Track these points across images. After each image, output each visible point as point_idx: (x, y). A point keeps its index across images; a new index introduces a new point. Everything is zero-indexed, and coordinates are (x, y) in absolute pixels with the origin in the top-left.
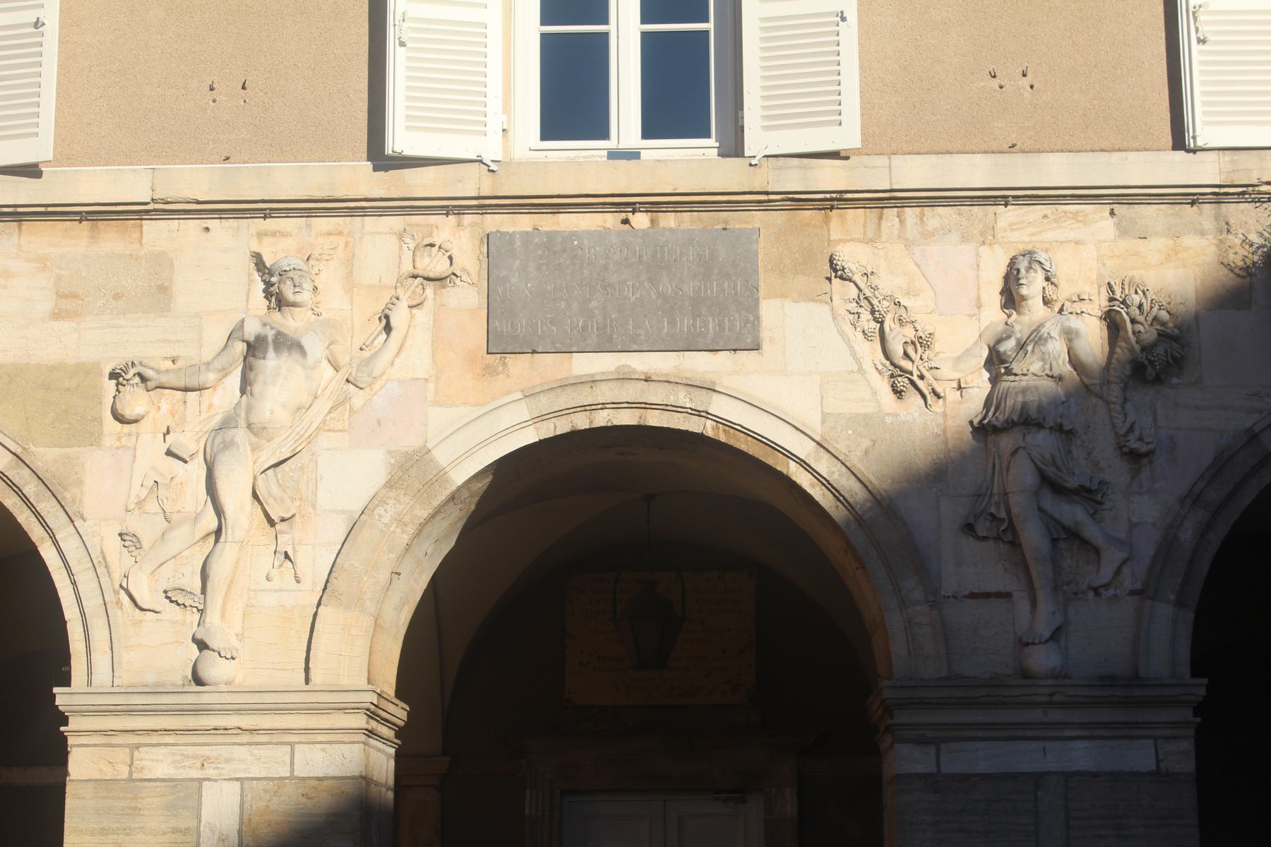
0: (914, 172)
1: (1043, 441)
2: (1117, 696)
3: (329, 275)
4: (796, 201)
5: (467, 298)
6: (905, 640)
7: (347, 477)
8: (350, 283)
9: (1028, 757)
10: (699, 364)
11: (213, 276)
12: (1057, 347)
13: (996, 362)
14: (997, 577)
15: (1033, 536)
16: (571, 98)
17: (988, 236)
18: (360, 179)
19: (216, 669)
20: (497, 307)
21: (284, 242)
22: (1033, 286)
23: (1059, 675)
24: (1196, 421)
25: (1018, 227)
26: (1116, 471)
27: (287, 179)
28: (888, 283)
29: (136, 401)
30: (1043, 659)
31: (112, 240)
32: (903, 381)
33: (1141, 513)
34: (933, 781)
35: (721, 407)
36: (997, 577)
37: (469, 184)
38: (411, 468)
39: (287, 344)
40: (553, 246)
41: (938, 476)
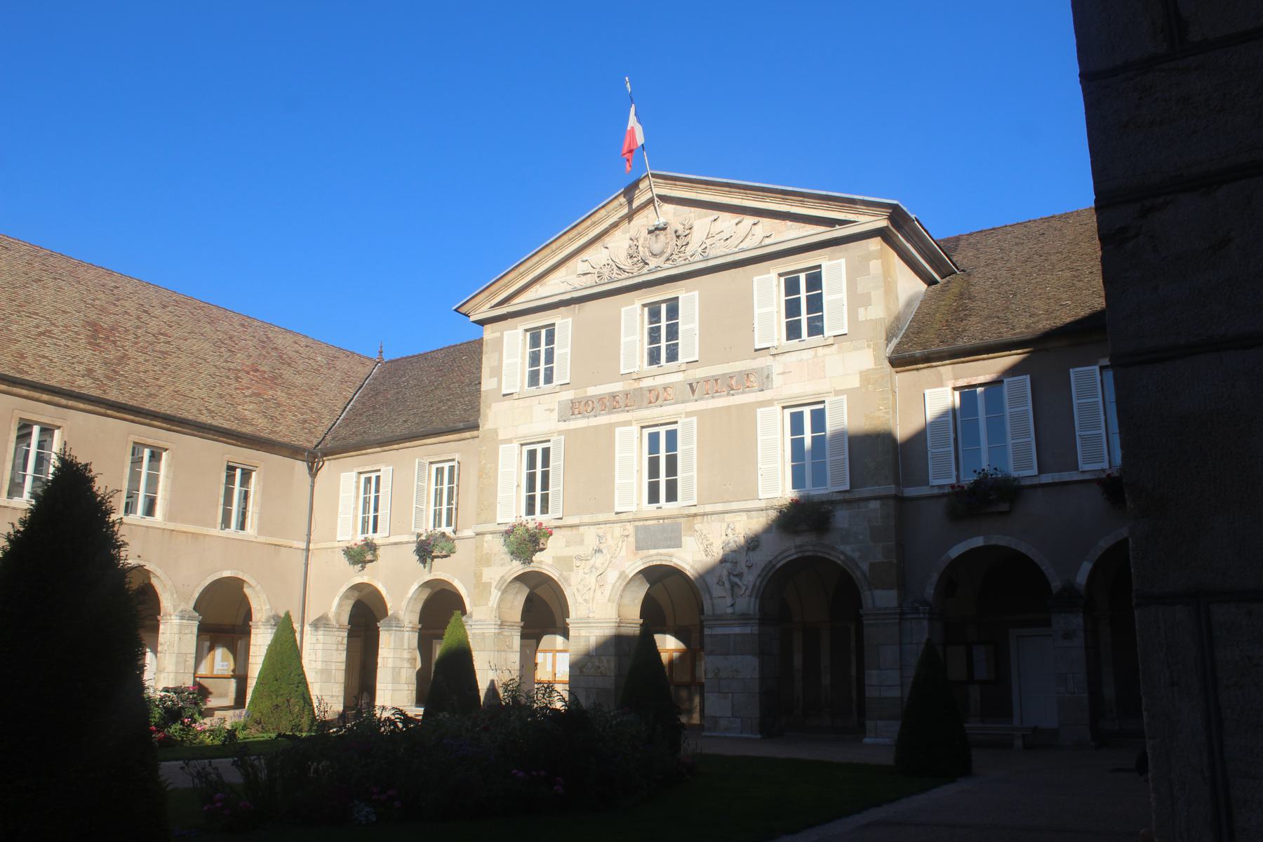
0: (708, 508)
1: (728, 565)
2: (744, 618)
3: (609, 536)
4: (688, 516)
5: (632, 539)
7: (612, 577)
10: (671, 551)
15: (727, 585)
16: (653, 497)
20: (637, 541)
23: (733, 613)
24: (761, 558)
26: (745, 570)
27: (602, 517)
30: (729, 610)
33: (750, 578)
34: (710, 636)
36: (723, 594)
37: (631, 517)
38: (622, 574)
40: (646, 527)
41: (711, 571)
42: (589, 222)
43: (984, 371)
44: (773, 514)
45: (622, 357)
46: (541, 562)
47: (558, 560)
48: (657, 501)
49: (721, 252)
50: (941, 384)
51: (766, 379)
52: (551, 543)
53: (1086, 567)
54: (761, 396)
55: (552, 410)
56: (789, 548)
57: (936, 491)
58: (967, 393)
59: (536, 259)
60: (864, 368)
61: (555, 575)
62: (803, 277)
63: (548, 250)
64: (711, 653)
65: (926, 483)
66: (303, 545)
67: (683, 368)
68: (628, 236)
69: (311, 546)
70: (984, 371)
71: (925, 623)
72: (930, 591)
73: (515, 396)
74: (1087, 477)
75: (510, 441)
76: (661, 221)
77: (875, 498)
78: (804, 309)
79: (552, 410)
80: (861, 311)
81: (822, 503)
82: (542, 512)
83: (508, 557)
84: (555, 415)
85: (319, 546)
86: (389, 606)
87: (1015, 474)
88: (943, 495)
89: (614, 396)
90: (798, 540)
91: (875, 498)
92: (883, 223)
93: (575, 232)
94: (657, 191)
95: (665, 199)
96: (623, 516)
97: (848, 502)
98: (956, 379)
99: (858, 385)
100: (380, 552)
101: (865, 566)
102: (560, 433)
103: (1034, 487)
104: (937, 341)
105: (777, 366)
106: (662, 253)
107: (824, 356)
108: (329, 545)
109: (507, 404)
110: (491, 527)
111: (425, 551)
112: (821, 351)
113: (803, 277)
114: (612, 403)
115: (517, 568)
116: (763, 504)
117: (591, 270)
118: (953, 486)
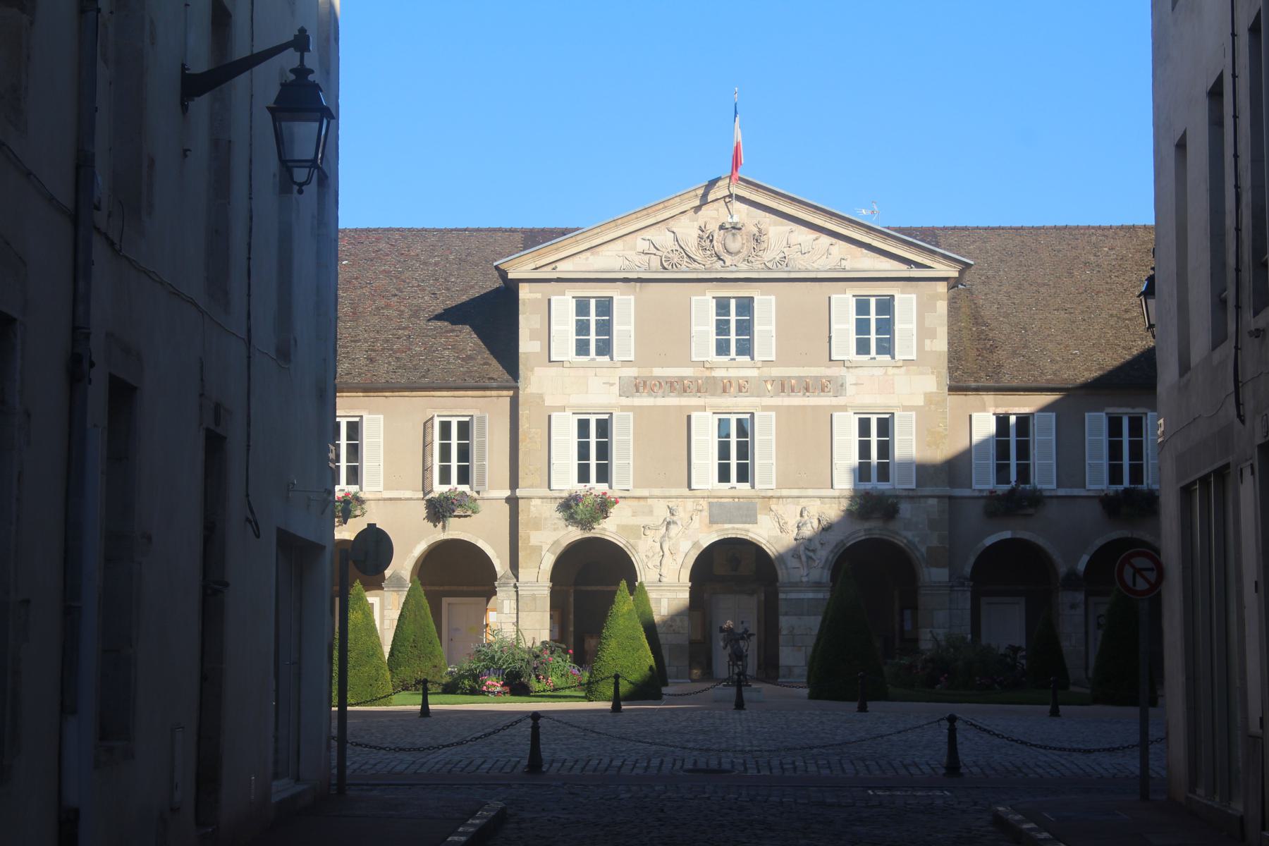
0: (785, 492)
2: (817, 585)
3: (680, 509)
4: (764, 497)
5: (706, 514)
6: (782, 574)
8: (685, 510)
9: (801, 596)
10: (747, 526)
11: (660, 511)
14: (798, 565)
15: (804, 558)
16: (724, 475)
18: (686, 491)
19: (663, 579)
22: (805, 514)
24: (834, 538)
25: (803, 502)
26: (819, 546)
27: (674, 492)
29: (648, 532)
30: (805, 579)
31: (642, 502)
33: (823, 554)
36: (798, 565)
37: (706, 494)
38: (695, 544)
39: (675, 523)
40: (721, 505)
44: (845, 504)
45: (693, 345)
46: (604, 529)
47: (622, 528)
48: (729, 481)
50: (984, 409)
51: (838, 387)
52: (614, 511)
53: (1085, 559)
55: (612, 385)
56: (861, 531)
57: (976, 494)
60: (928, 390)
61: (620, 541)
62: (873, 301)
63: (613, 224)
64: (786, 614)
65: (970, 487)
67: (759, 365)
68: (696, 225)
71: (969, 594)
72: (968, 570)
73: (566, 364)
74: (1091, 494)
75: (563, 409)
76: (735, 219)
78: (877, 330)
79: (612, 385)
80: (927, 342)
81: (890, 496)
82: (599, 480)
83: (563, 523)
84: (616, 389)
87: (1039, 487)
88: (982, 497)
89: (682, 379)
90: (867, 525)
92: (956, 275)
96: (697, 493)
97: (911, 498)
98: (997, 406)
99: (922, 404)
101: (924, 550)
102: (624, 408)
103: (1051, 497)
104: (982, 374)
105: (850, 377)
109: (553, 371)
111: (438, 510)
112: (891, 371)
113: (873, 301)
116: (836, 493)
118: (991, 492)
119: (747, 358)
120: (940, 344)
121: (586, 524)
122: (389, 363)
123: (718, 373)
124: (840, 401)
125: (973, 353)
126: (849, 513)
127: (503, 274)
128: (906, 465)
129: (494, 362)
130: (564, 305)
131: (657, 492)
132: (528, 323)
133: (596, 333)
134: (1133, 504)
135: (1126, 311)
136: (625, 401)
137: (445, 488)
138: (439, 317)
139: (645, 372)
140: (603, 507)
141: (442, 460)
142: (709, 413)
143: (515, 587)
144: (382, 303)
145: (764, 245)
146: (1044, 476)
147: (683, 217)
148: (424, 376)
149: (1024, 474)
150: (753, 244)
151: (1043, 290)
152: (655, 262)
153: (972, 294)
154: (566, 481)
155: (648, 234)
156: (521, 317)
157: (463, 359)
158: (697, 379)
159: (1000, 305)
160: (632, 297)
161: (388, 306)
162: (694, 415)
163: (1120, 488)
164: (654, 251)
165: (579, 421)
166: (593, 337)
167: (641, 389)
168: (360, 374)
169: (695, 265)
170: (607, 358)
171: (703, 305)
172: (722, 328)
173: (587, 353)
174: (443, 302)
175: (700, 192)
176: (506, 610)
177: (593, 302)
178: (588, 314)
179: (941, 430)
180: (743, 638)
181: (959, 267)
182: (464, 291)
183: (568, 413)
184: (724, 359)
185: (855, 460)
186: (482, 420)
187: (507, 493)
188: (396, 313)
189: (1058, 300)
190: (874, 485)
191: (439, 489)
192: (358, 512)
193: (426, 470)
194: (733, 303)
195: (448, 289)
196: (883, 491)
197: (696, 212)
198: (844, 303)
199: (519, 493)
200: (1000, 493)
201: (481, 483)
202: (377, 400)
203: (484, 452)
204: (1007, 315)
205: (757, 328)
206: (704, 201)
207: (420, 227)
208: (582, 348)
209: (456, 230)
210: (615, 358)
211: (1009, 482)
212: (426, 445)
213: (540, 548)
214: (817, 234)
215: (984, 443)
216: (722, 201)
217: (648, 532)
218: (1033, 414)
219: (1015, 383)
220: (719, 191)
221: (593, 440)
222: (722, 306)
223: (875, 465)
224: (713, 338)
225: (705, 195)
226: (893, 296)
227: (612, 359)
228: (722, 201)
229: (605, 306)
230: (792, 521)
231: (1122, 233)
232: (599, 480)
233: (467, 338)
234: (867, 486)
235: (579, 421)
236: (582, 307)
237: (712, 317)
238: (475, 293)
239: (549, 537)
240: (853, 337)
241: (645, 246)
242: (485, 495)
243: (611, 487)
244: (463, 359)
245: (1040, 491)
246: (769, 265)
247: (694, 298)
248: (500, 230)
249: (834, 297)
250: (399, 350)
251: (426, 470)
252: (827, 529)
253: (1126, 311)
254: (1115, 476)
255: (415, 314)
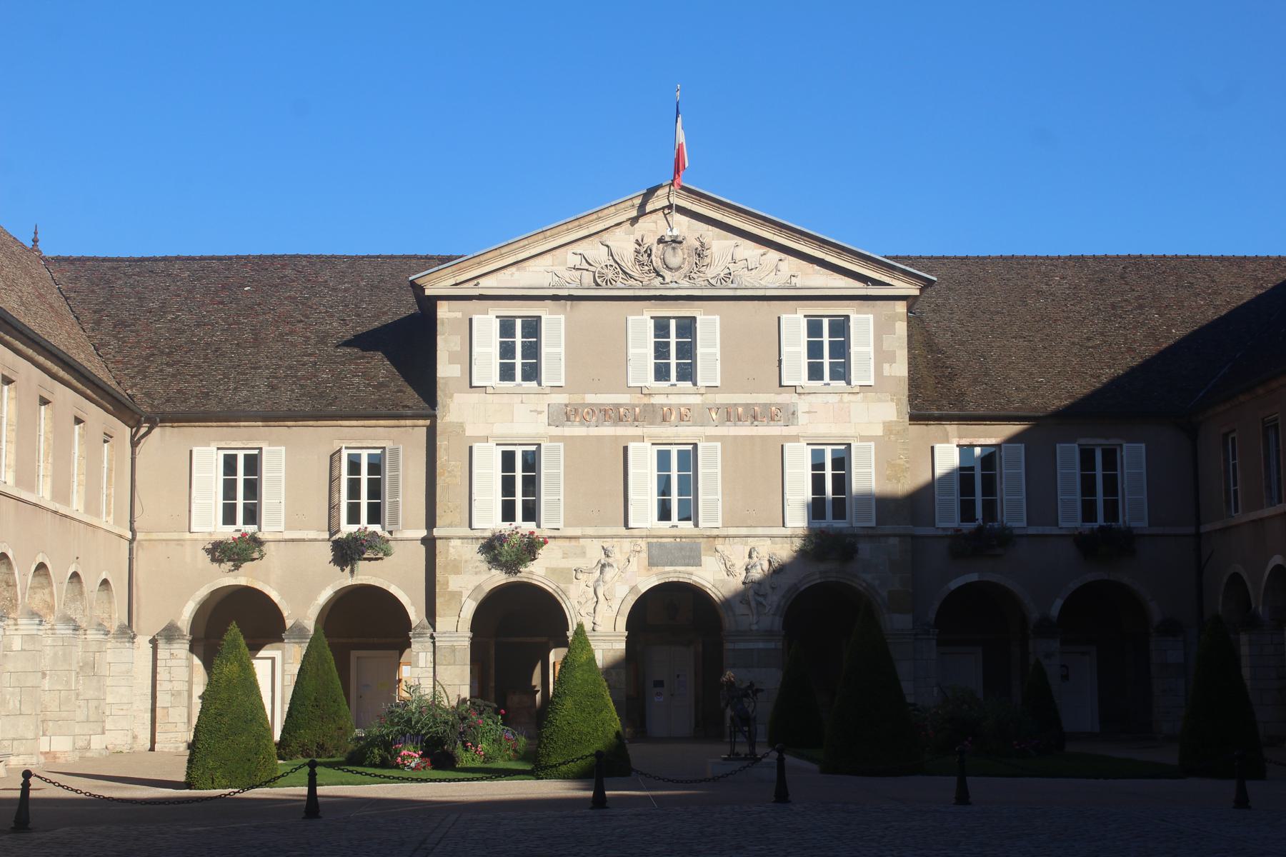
0: (732, 531)
3: (616, 550)
4: (709, 537)
5: (644, 555)
6: (728, 623)
9: (751, 646)
10: (690, 569)
11: (594, 552)
12: (759, 567)
13: (747, 569)
15: (753, 604)
16: (664, 514)
17: (746, 544)
18: (623, 531)
19: (597, 628)
21: (608, 544)
22: (754, 555)
27: (608, 531)
28: (726, 553)
29: (580, 576)
30: (755, 627)
31: (573, 543)
32: (729, 573)
33: (774, 599)
35: (694, 578)
37: (644, 533)
38: (633, 589)
40: (661, 545)
42: (595, 216)
43: (992, 435)
44: (798, 543)
45: (630, 369)
46: (531, 573)
47: (552, 571)
49: (750, 282)
50: (946, 440)
52: (542, 553)
53: (1059, 603)
54: (786, 431)
55: (540, 413)
56: (816, 574)
57: (940, 533)
58: (965, 450)
59: (525, 242)
61: (549, 586)
62: (826, 322)
63: (541, 236)
66: (129, 535)
67: (703, 391)
68: (633, 239)
69: (139, 536)
70: (992, 435)
72: (932, 616)
75: (486, 439)
76: (675, 232)
77: (895, 535)
78: (831, 353)
79: (540, 413)
80: (886, 366)
82: (525, 519)
83: (485, 566)
85: (154, 536)
86: (285, 614)
88: (947, 536)
89: (617, 406)
91: (895, 535)
92: (917, 292)
93: (577, 223)
94: (676, 201)
95: (682, 210)
96: (635, 532)
97: (871, 537)
100: (264, 548)
102: (553, 439)
105: (802, 404)
106: (680, 267)
107: (850, 402)
108: (175, 536)
109: (475, 397)
110: (465, 531)
111: (346, 553)
113: (826, 322)
114: (613, 414)
115: (498, 578)
116: (788, 532)
117: (585, 266)
118: (957, 530)
119: (689, 384)
120: (900, 369)
121: (511, 566)
122: (292, 391)
123: (657, 400)
124: (791, 431)
125: (932, 381)
126: (802, 554)
127: (418, 289)
128: (865, 498)
129: (409, 390)
130: (487, 324)
131: (590, 531)
132: (447, 345)
133: (523, 355)
134: (1106, 543)
135: (1089, 339)
136: (554, 431)
137: (353, 528)
138: (348, 344)
139: (577, 399)
140: (531, 548)
141: (350, 497)
142: (647, 444)
143: (432, 637)
144: (287, 329)
145: (707, 261)
146: (1013, 509)
147: (618, 230)
148: (331, 404)
149: (990, 508)
150: (695, 259)
151: (997, 318)
152: (588, 278)
153: (922, 321)
154: (489, 519)
155: (578, 248)
156: (439, 339)
157: (374, 386)
158: (634, 406)
159: (954, 334)
160: (562, 317)
161: (291, 333)
162: (631, 446)
163: (1096, 525)
164: (587, 266)
165: (504, 453)
166: (518, 361)
167: (572, 418)
168: (259, 402)
169: (632, 282)
170: (534, 384)
171: (641, 324)
172: (661, 350)
173: (512, 378)
174: (353, 328)
175: (638, 201)
176: (422, 663)
177: (519, 323)
178: (513, 336)
179: (901, 462)
180: (747, 695)
181: (920, 284)
182: (377, 317)
183: (492, 444)
184: (663, 385)
185: (808, 495)
186: (395, 452)
187: (424, 533)
188: (301, 340)
189: (1015, 328)
190: (829, 522)
191: (346, 529)
192: (256, 555)
193: (333, 508)
194: (673, 323)
195: (358, 315)
196: (841, 529)
197: (632, 225)
198: (795, 323)
199: (436, 532)
200: (965, 531)
201: (395, 521)
202: (279, 431)
203: (397, 487)
204: (962, 343)
205: (700, 350)
206: (642, 212)
207: (329, 254)
208: (507, 373)
209: (368, 257)
210: (543, 383)
211: (973, 519)
212: (333, 480)
213: (460, 594)
214: (763, 249)
215: (947, 476)
216: (660, 213)
217: (580, 576)
218: (998, 446)
219: (981, 412)
220: (658, 202)
221: (519, 474)
222: (661, 327)
223: (834, 498)
224: (651, 362)
225: (642, 206)
226: (847, 317)
227: (540, 384)
228: (660, 213)
229: (533, 327)
230: (740, 562)
231: (1071, 263)
232: (525, 519)
233: (380, 365)
234: (823, 524)
235: (504, 453)
236: (507, 327)
237: (651, 340)
238: (388, 319)
239: (471, 580)
240: (804, 361)
241: (576, 261)
242: (397, 535)
243: (539, 526)
244: (374, 386)
245: (1011, 529)
246: (713, 282)
247: (630, 318)
248: (415, 257)
249: (784, 317)
250: (303, 377)
251: (333, 508)
252: (778, 571)
253: (1089, 339)
254: (1088, 512)
255: (322, 340)
